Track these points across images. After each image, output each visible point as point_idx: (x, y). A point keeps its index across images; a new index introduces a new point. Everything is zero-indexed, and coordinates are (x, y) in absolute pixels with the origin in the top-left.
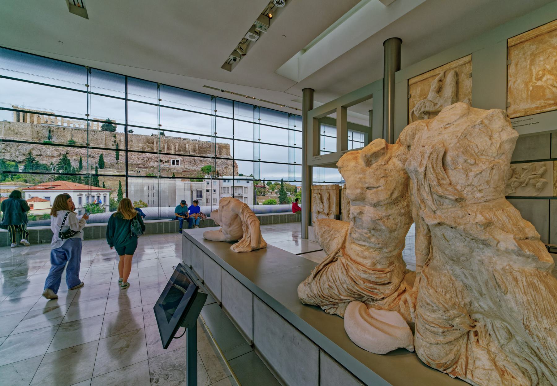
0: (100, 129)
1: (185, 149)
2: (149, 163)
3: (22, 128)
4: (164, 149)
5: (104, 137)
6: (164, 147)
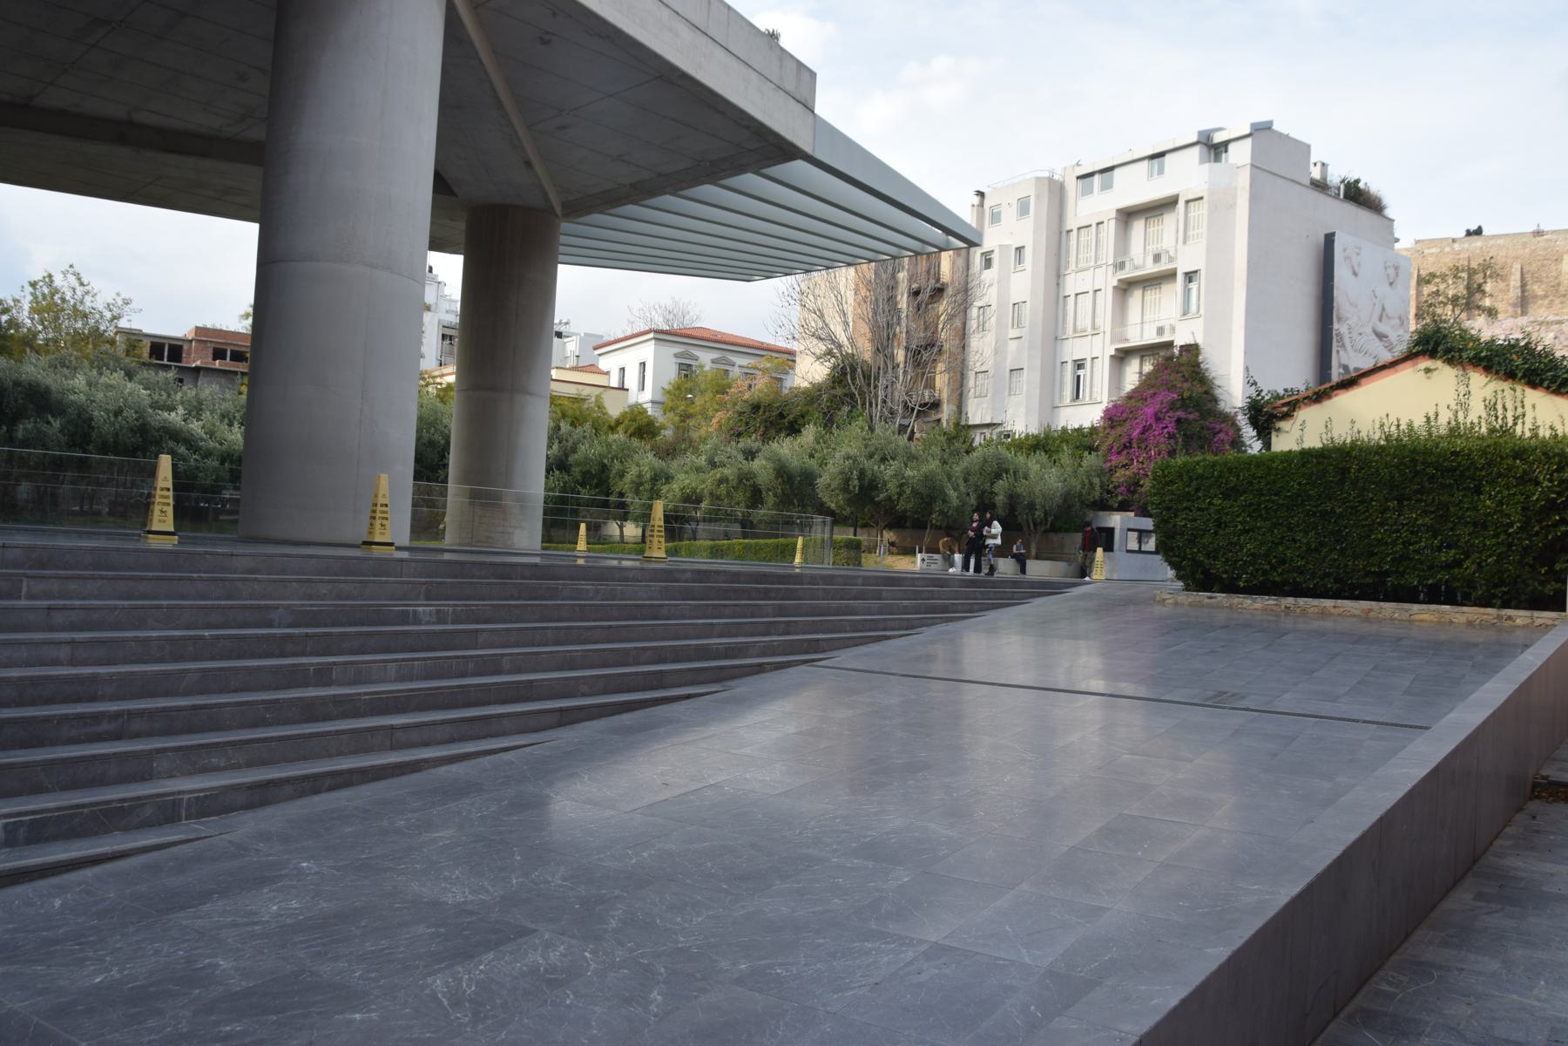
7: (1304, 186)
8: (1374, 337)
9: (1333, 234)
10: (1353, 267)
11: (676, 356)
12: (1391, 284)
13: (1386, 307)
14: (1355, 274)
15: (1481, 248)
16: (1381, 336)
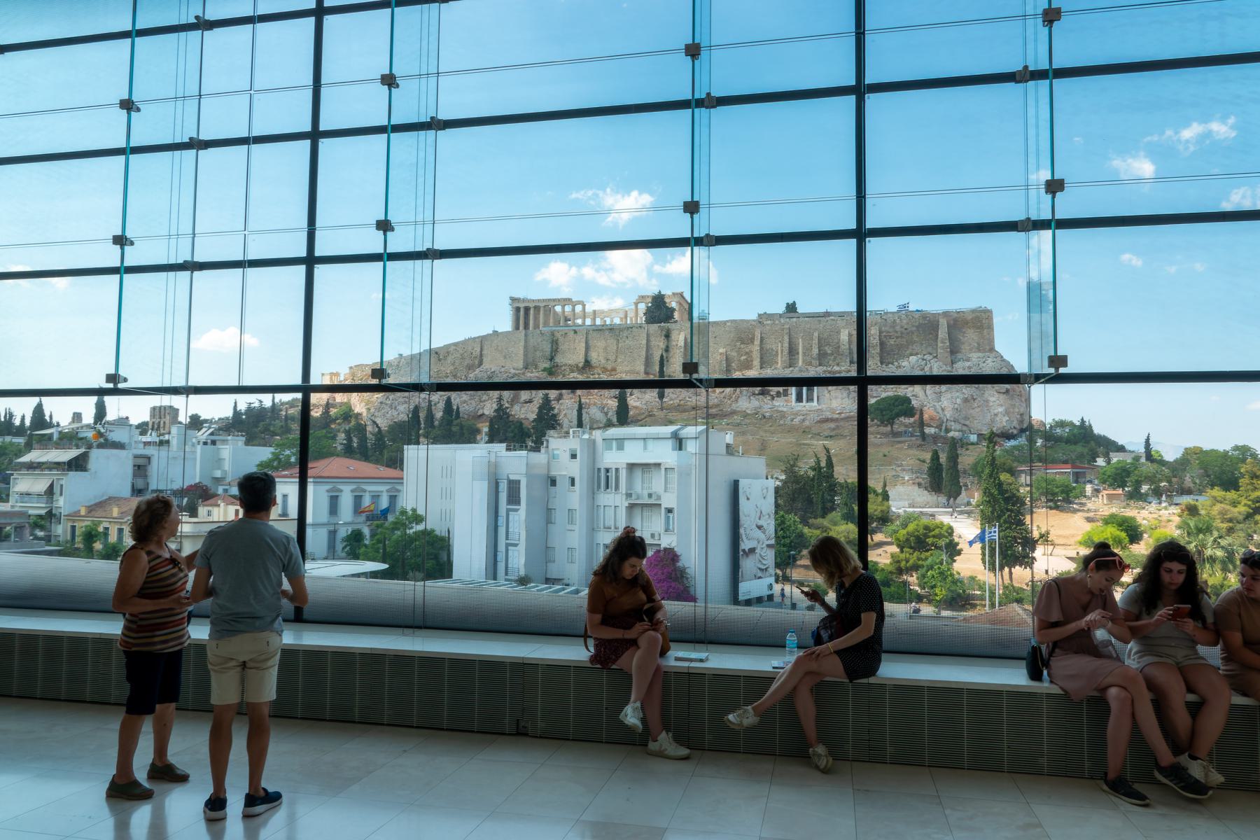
0: (642, 319)
1: (839, 347)
3: (513, 343)
5: (644, 342)
7: (722, 455)
8: (757, 529)
9: (738, 481)
10: (747, 496)
11: (328, 491)
12: (764, 498)
13: (763, 512)
14: (748, 499)
15: (796, 322)
16: (760, 527)
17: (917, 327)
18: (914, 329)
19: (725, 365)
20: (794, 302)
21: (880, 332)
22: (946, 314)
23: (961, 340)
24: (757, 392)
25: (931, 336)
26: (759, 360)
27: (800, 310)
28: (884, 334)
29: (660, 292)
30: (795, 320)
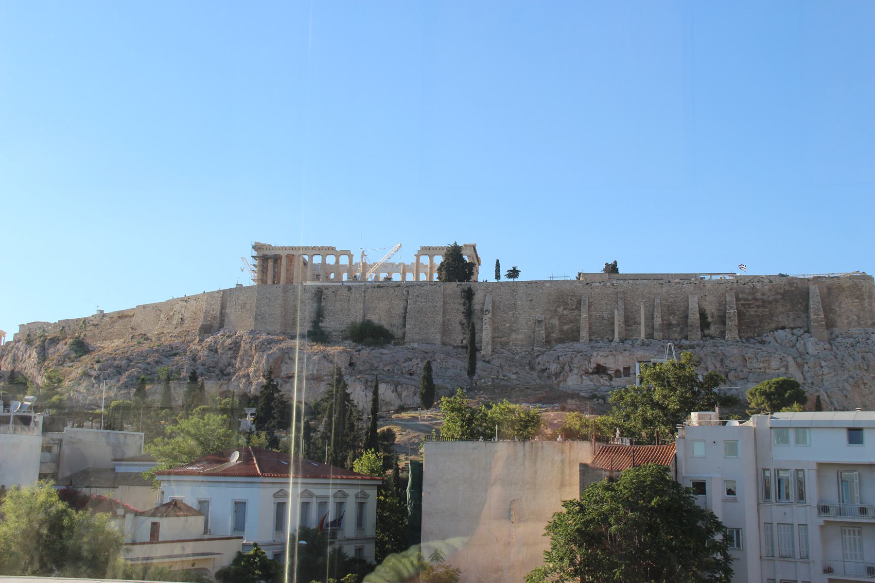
1: (687, 317)
2: (565, 380)
4: (613, 324)
5: (440, 304)
6: (613, 318)
17: (783, 295)
18: (780, 297)
19: (544, 335)
20: (615, 262)
21: (738, 299)
22: (817, 279)
23: (836, 311)
24: (590, 370)
25: (799, 306)
26: (587, 329)
27: (622, 270)
28: (742, 302)
29: (456, 243)
30: (631, 282)
